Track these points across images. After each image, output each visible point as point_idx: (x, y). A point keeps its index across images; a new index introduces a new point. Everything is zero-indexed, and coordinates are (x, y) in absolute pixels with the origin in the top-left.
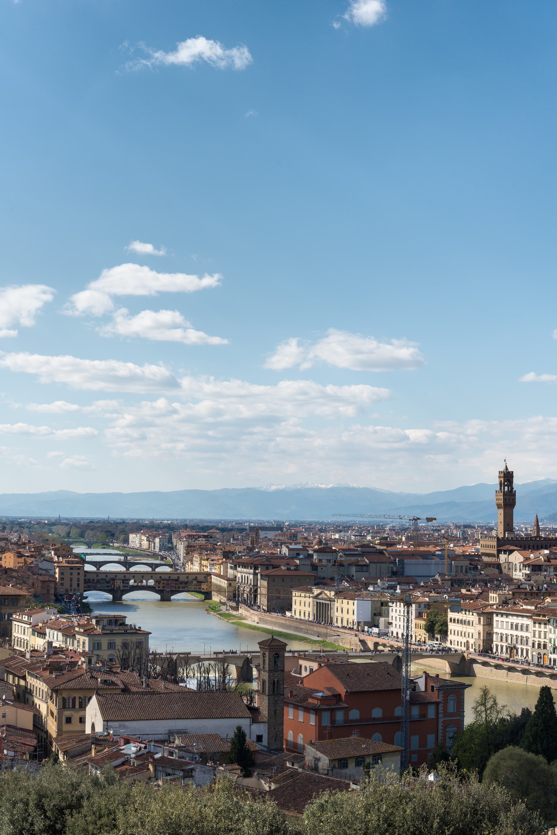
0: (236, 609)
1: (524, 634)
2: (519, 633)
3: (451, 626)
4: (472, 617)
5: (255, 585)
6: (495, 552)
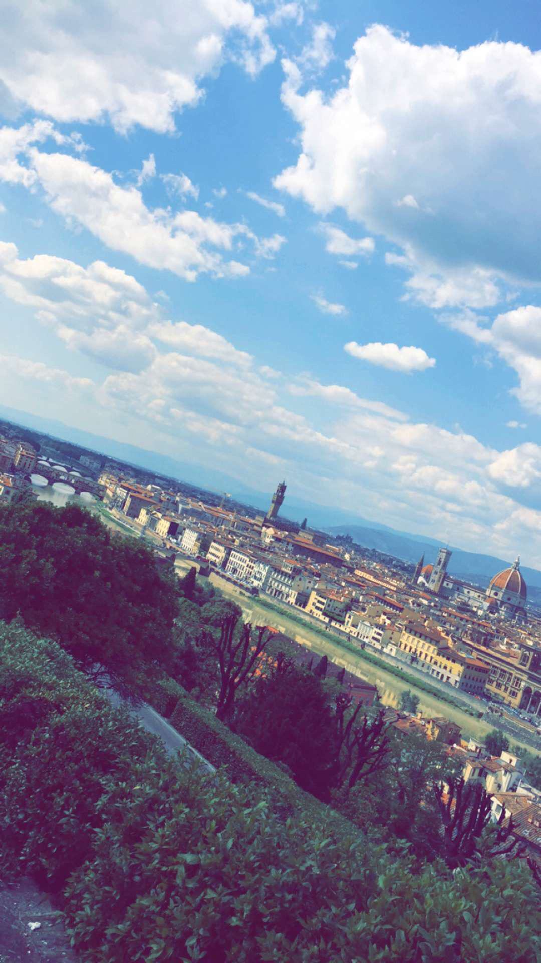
0: (111, 509)
1: (244, 564)
2: (241, 563)
3: (211, 550)
4: (222, 548)
5: (125, 500)
6: (261, 524)
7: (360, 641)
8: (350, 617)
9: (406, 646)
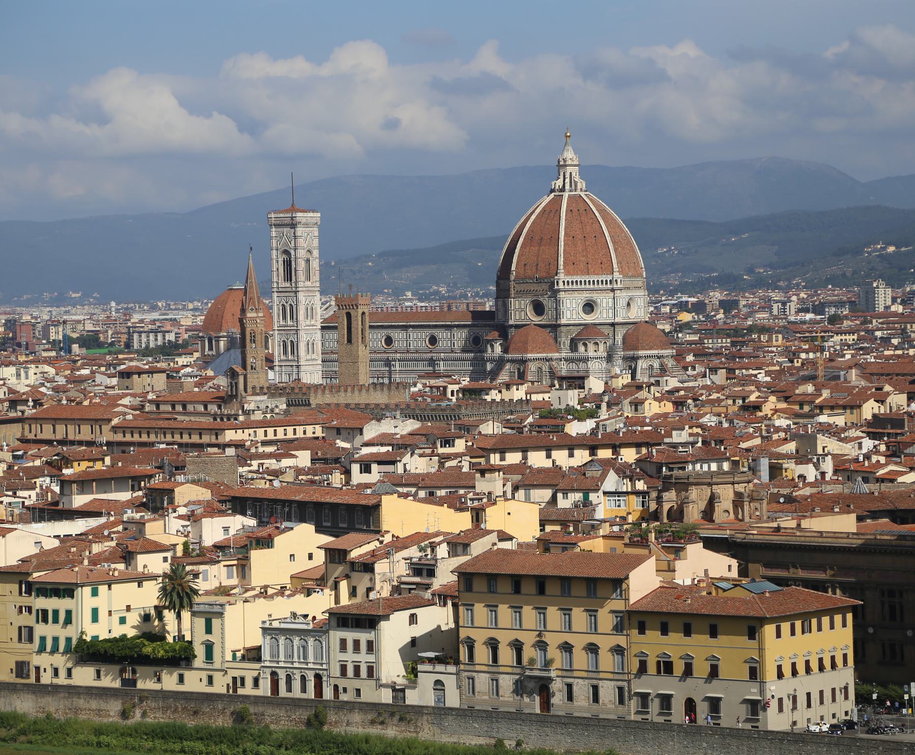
7: (296, 703)
8: (209, 630)
9: (493, 645)
